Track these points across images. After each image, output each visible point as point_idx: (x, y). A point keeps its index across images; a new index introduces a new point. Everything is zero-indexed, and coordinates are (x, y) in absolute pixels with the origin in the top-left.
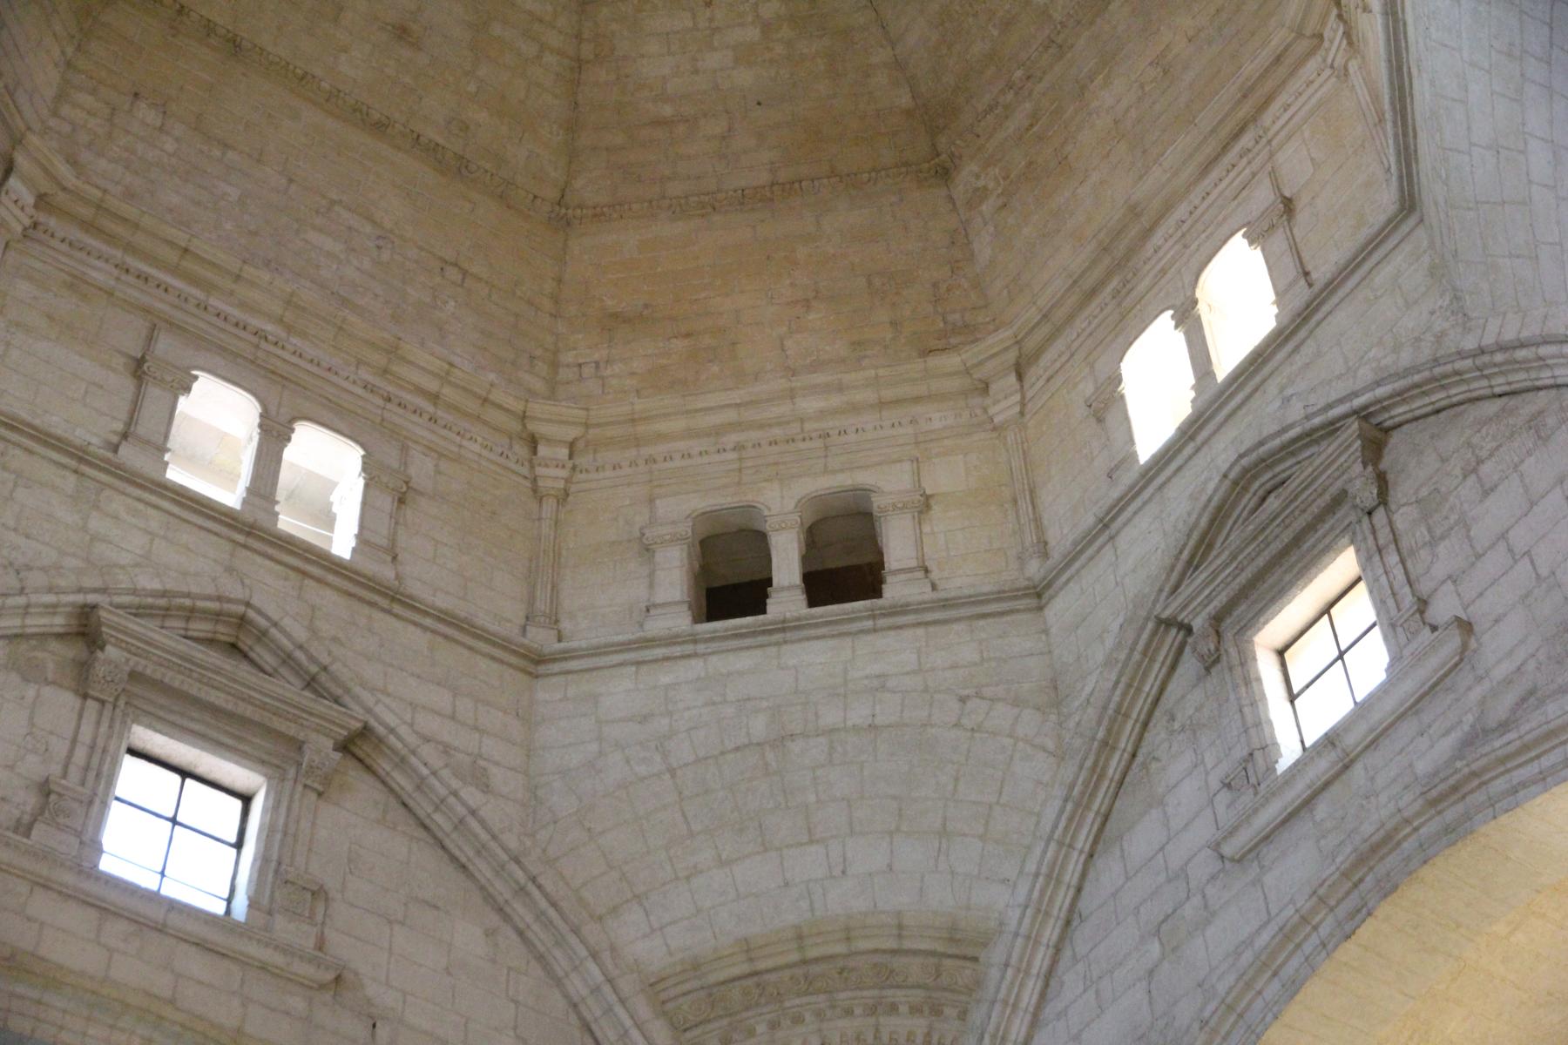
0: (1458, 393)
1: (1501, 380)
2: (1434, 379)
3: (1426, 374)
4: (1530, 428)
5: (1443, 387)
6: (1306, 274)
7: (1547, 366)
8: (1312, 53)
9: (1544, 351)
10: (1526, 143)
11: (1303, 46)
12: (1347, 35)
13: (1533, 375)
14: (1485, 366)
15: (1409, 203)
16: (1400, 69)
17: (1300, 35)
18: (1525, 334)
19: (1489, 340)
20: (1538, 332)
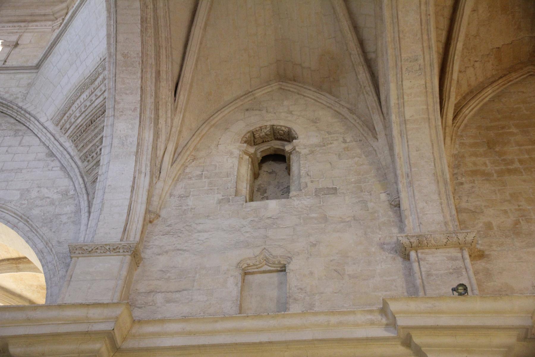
0: (9, 112)
1: (19, 117)
2: (7, 105)
3: (6, 103)
4: (15, 131)
5: (8, 108)
6: (5, 61)
7: (30, 122)
8: (53, 20)
9: (32, 118)
10: (65, 75)
11: (52, 17)
13: (26, 122)
15: (38, 67)
16: (58, 38)
17: (53, 15)
18: (32, 112)
19: (24, 107)
20: (34, 114)
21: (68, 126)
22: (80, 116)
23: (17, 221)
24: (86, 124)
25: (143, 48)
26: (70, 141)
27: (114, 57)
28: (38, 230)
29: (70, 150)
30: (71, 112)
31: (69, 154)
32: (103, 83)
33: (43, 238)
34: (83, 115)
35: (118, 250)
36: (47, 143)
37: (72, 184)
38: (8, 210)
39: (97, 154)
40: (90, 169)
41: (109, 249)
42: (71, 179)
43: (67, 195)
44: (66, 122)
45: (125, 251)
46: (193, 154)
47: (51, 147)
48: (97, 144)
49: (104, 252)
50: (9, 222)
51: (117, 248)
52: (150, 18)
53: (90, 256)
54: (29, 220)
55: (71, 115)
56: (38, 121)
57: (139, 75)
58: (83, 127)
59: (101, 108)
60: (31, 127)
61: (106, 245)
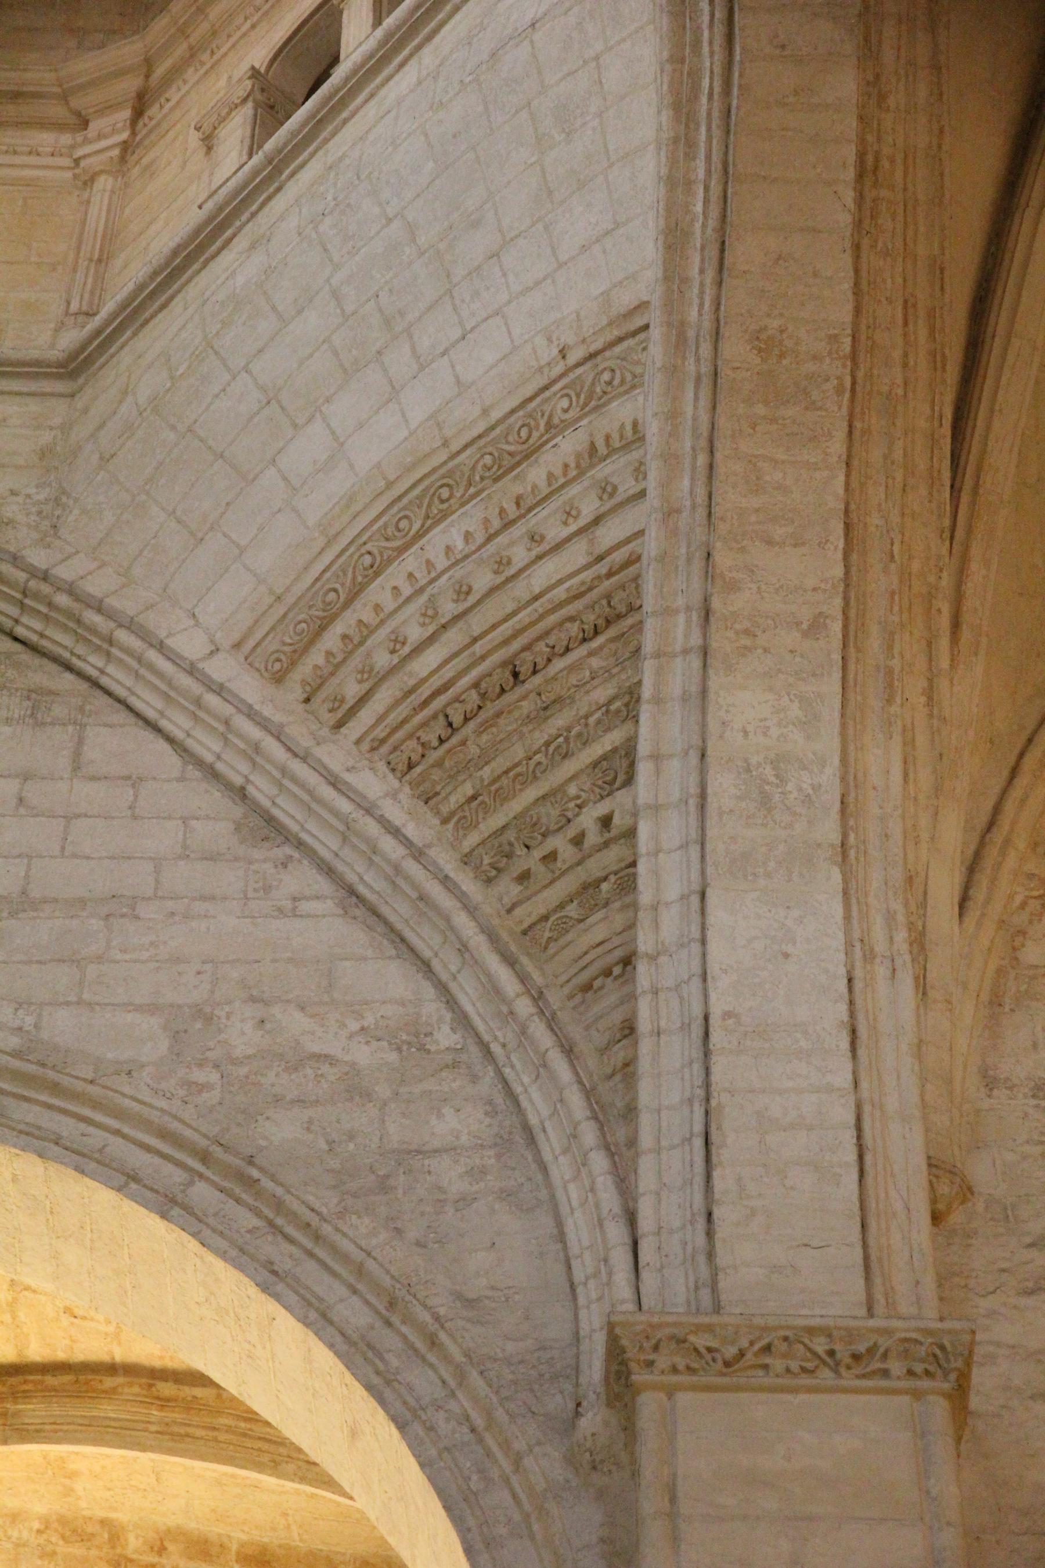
1: (38, 625)
4: (29, 698)
7: (108, 654)
8: (60, 127)
9: (122, 636)
10: (310, 420)
11: (57, 111)
12: (126, 147)
13: (80, 649)
14: (37, 596)
17: (64, 98)
18: (112, 602)
19: (65, 573)
20: (131, 613)
21: (352, 690)
22: (431, 639)
23: (179, 1176)
24: (476, 685)
25: (858, 311)
26: (382, 766)
27: (706, 349)
28: (327, 1229)
29: (395, 814)
30: (362, 611)
31: (395, 832)
32: (582, 473)
33: (360, 1271)
34: (454, 637)
35: (877, 1365)
36: (236, 769)
37: (429, 991)
38: (120, 1114)
39: (578, 841)
40: (545, 918)
41: (831, 1353)
42: (426, 967)
43: (422, 1048)
44: (338, 666)
45: (919, 1368)
46: (1030, 867)
47: (261, 789)
48: (572, 790)
49: (804, 1370)
50: (135, 1178)
51: (871, 1351)
52: (892, 161)
53: (738, 1389)
54: (255, 1173)
55: (367, 630)
56: (161, 647)
57: (837, 446)
58: (457, 699)
59: (578, 605)
60: (117, 678)
61: (811, 1331)
